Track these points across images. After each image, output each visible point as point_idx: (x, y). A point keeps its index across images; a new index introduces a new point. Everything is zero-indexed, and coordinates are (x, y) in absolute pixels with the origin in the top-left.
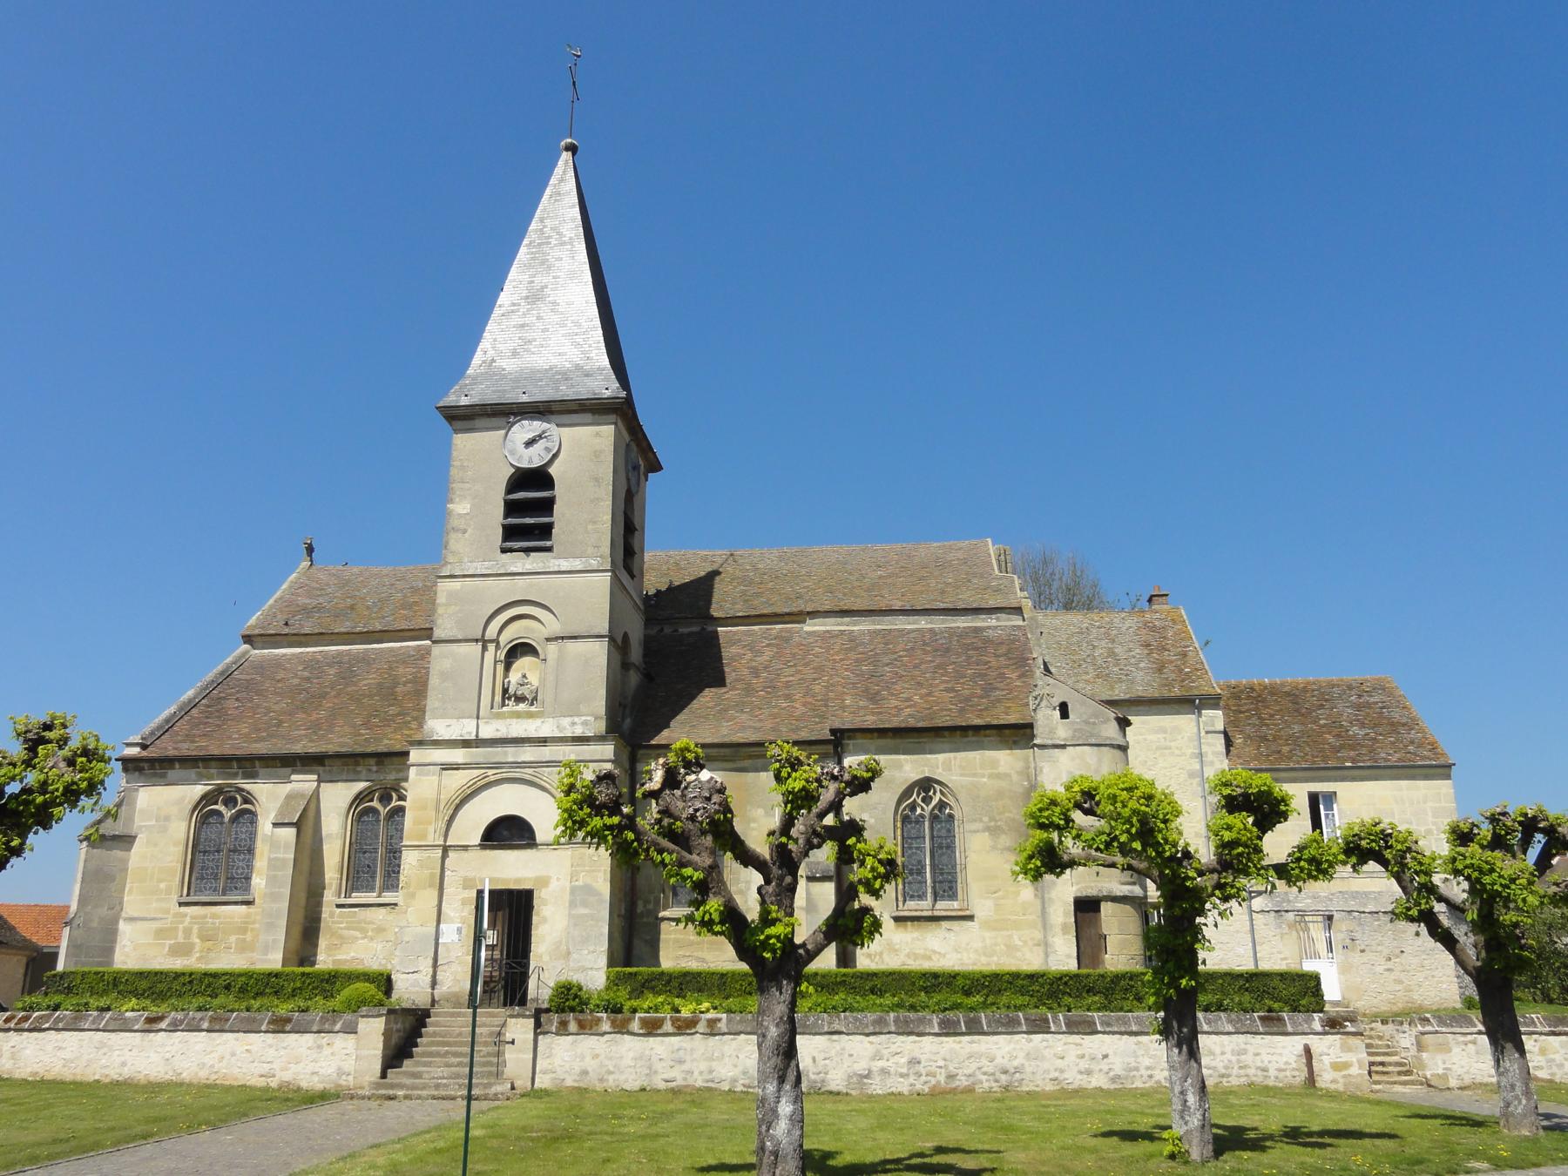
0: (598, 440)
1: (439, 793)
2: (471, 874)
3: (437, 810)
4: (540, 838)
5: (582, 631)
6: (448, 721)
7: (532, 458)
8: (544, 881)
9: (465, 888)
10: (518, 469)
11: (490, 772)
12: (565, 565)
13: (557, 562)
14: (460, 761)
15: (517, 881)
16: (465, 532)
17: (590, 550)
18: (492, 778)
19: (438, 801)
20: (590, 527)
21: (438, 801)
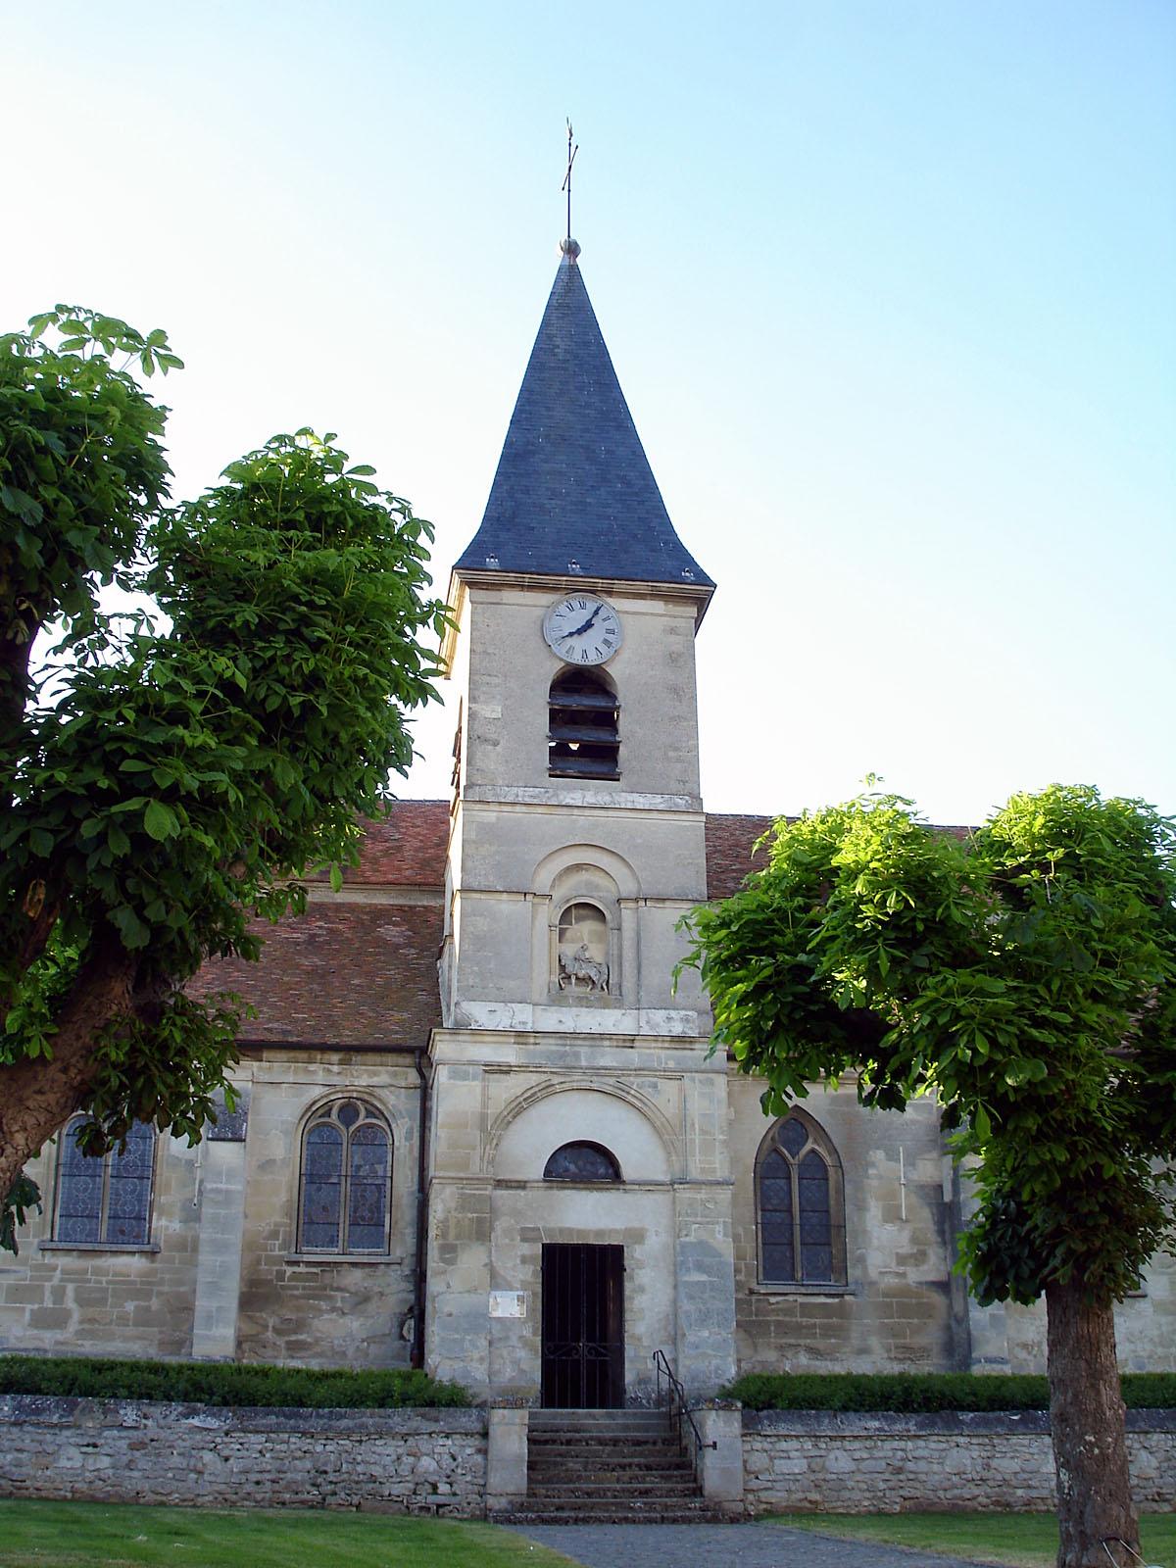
0: (673, 638)
1: (485, 1105)
4: (627, 1172)
5: (670, 892)
6: (493, 1006)
7: (585, 652)
8: (639, 1236)
10: (568, 664)
11: (556, 1080)
12: (641, 801)
13: (631, 797)
15: (600, 1233)
16: (496, 744)
17: (674, 786)
20: (671, 754)
21: (483, 1117)
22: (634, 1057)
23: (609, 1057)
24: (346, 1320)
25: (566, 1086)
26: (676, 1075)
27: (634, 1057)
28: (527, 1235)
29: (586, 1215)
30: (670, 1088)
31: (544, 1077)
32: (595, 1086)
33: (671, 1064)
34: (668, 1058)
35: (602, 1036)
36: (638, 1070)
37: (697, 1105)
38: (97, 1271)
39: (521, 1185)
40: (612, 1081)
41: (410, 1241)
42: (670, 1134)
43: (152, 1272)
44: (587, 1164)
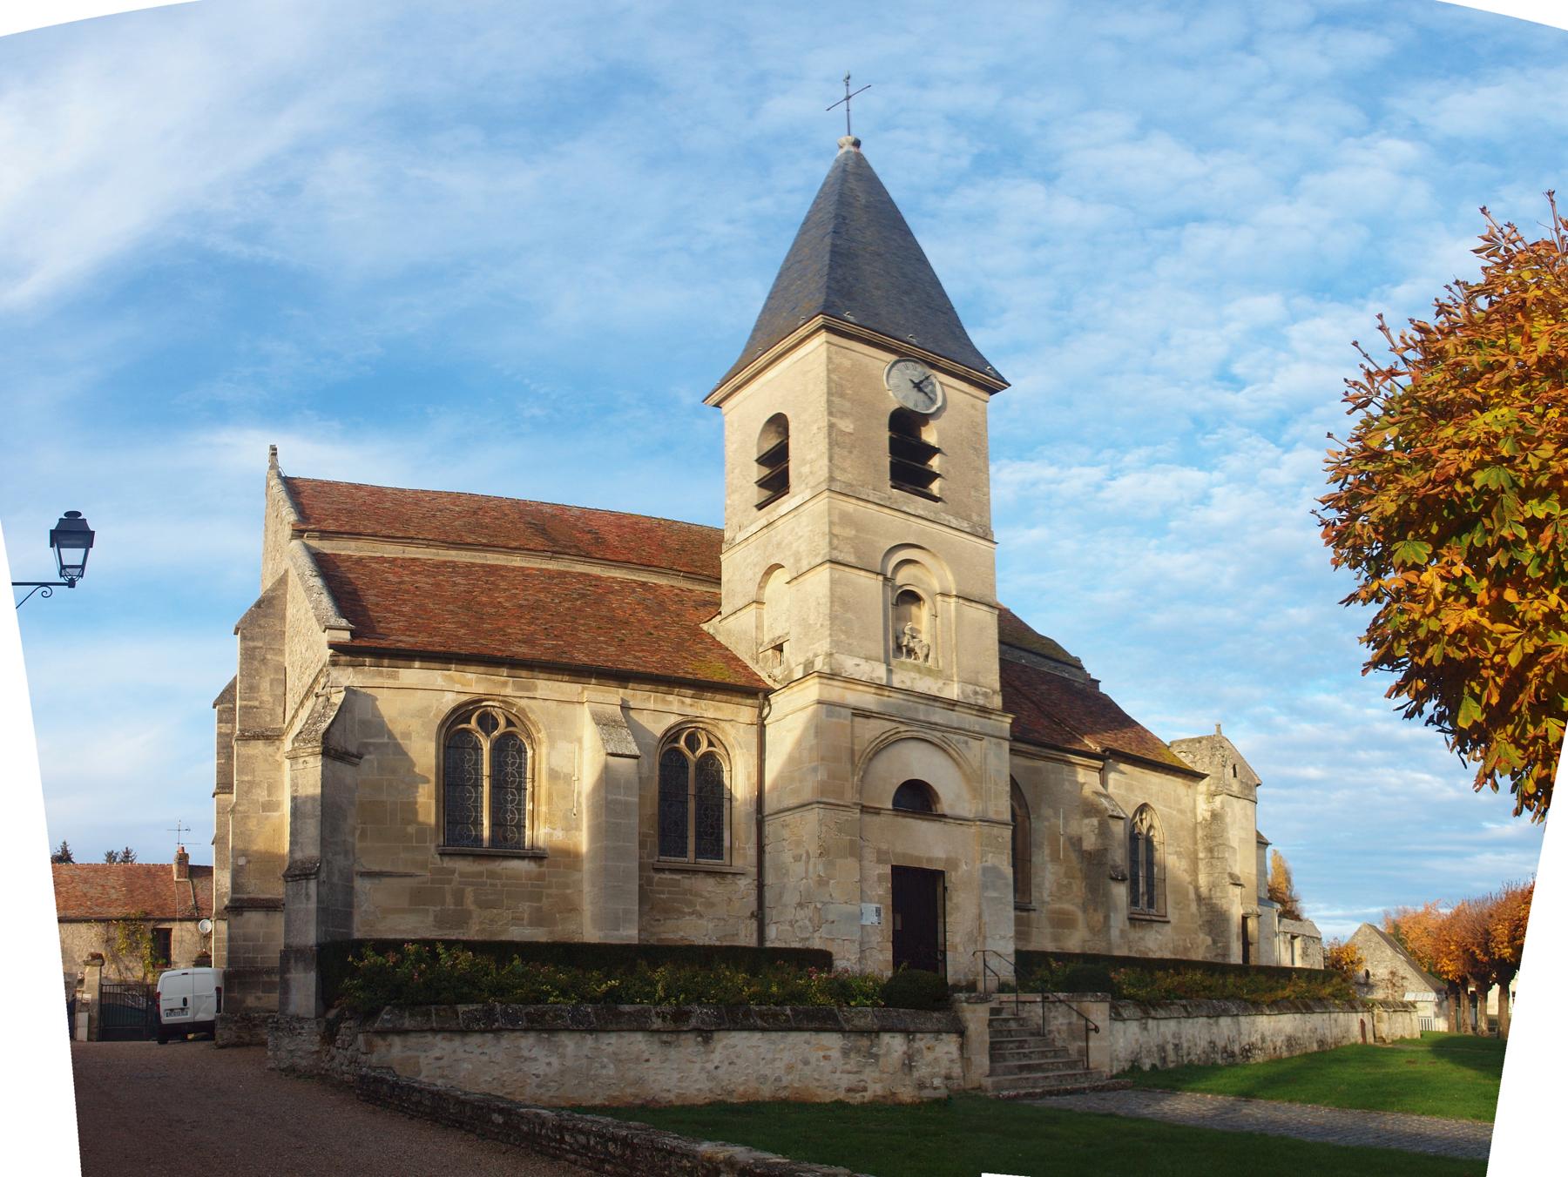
2: (884, 847)
3: (853, 763)
6: (857, 661)
8: (953, 863)
9: (879, 861)
11: (903, 728)
14: (873, 707)
15: (930, 860)
18: (904, 735)
19: (853, 752)
22: (954, 718)
23: (939, 716)
24: (703, 922)
25: (909, 735)
26: (979, 736)
27: (954, 718)
28: (881, 858)
29: (926, 843)
30: (974, 744)
31: (894, 725)
32: (928, 737)
33: (977, 728)
34: (971, 721)
35: (936, 699)
36: (957, 730)
37: (992, 761)
38: (492, 875)
39: (877, 811)
40: (939, 734)
41: (752, 852)
42: (975, 780)
43: (541, 877)
44: (916, 798)
